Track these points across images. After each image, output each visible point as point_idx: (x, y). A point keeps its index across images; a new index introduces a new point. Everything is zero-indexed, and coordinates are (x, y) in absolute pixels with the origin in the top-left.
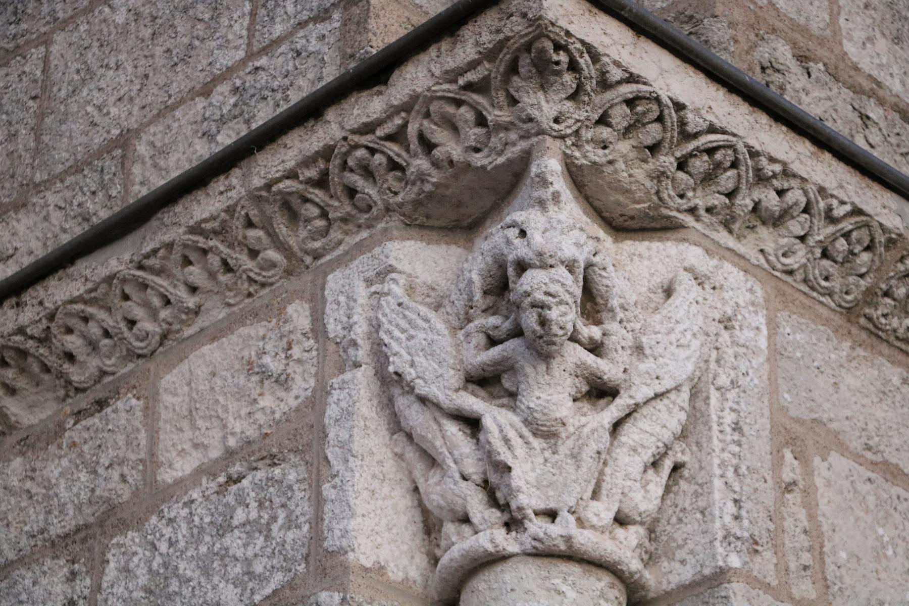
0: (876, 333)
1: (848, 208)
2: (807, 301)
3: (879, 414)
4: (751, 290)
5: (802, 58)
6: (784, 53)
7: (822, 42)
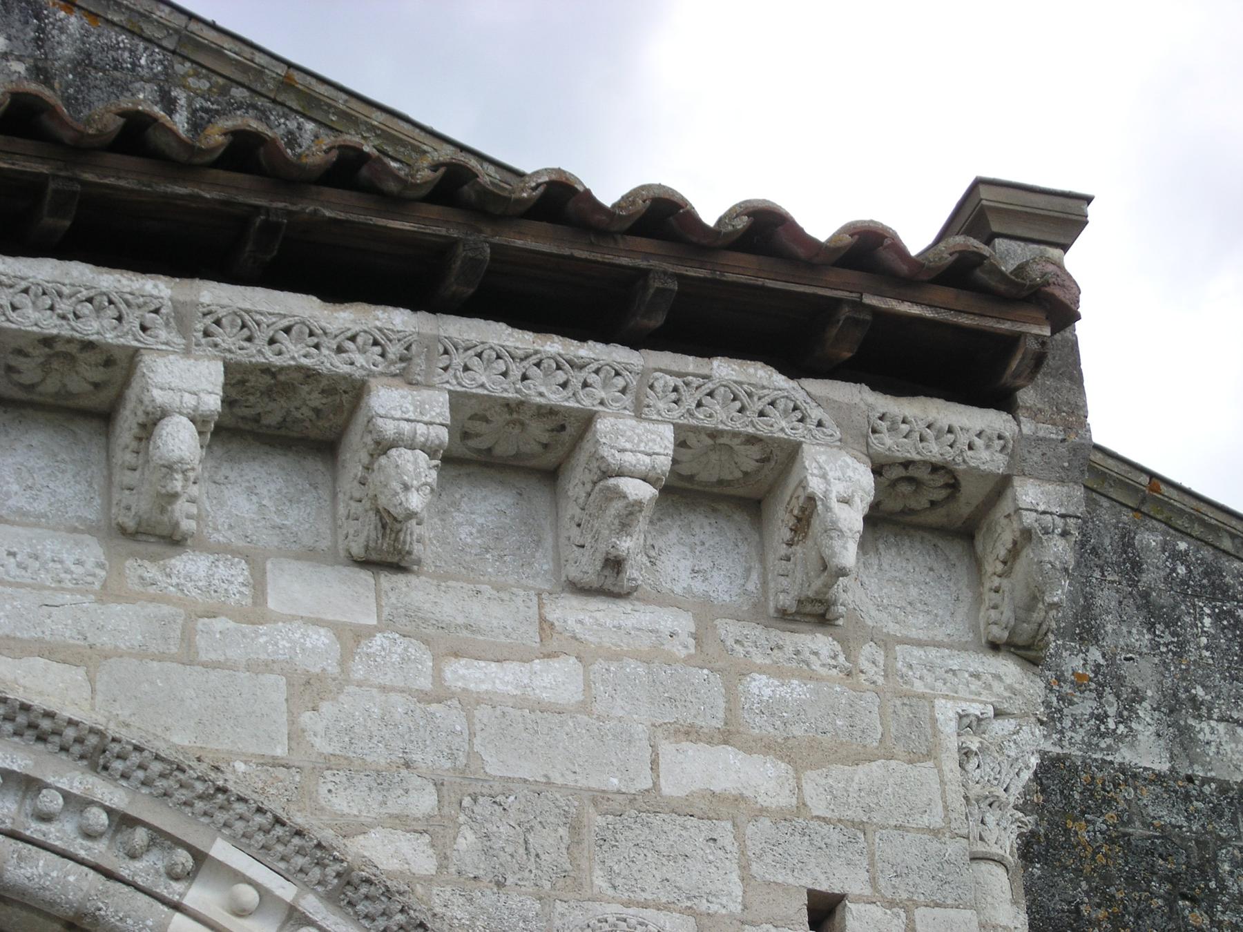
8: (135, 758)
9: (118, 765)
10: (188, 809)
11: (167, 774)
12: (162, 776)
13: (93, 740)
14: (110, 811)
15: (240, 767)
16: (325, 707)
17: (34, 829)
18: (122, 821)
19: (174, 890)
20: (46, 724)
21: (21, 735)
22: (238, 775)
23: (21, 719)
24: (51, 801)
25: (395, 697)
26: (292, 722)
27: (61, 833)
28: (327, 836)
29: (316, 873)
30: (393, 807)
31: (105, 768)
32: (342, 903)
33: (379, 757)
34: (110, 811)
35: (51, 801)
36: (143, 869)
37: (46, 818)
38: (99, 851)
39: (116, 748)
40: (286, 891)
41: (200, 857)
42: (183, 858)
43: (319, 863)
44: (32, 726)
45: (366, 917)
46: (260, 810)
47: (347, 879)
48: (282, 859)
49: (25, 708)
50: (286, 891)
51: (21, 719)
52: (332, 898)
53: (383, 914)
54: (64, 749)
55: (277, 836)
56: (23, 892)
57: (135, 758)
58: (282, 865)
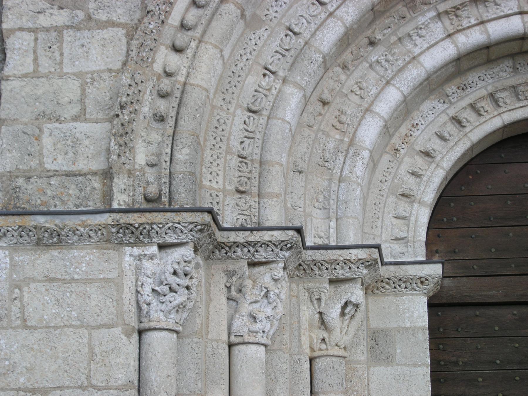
0: (47, 245)
1: (17, 227)
2: (24, 248)
3: (48, 266)
4: (5, 253)
5: (28, 178)
6: (21, 181)
7: (35, 170)
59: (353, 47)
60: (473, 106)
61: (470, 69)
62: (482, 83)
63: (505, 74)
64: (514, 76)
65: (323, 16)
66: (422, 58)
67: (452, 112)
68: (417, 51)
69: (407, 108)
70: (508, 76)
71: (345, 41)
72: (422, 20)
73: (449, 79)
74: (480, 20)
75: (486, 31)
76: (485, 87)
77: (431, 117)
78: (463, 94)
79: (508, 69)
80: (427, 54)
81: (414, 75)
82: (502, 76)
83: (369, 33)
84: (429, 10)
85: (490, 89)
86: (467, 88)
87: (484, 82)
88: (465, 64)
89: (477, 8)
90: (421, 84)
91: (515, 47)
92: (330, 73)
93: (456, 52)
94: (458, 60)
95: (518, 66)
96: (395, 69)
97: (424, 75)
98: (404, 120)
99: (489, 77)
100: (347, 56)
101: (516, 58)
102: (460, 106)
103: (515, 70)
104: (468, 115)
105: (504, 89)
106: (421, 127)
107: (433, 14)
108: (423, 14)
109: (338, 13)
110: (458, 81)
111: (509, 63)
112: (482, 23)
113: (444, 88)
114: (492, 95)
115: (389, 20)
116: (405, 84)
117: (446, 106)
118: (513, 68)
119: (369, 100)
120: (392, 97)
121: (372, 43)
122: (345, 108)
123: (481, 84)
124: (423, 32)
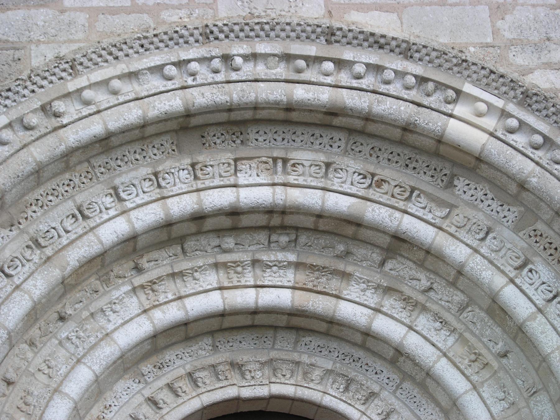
8: (424, 51)
9: (417, 55)
10: (450, 71)
11: (438, 56)
12: (437, 57)
13: (404, 45)
14: (416, 76)
15: (472, 49)
16: (508, 17)
17: (383, 88)
18: (422, 80)
19: (448, 108)
20: (382, 41)
21: (372, 47)
22: (472, 53)
23: (371, 40)
24: (389, 75)
25: (539, 9)
26: (493, 26)
27: (395, 88)
28: (515, 76)
29: (512, 93)
30: (544, 60)
31: (411, 57)
32: (526, 106)
33: (535, 37)
34: (416, 76)
35: (389, 75)
36: (434, 100)
37: (387, 82)
38: (413, 94)
39: (415, 47)
40: (499, 103)
41: (458, 92)
42: (451, 93)
43: (513, 89)
44: (376, 42)
45: (537, 110)
46: (483, 68)
47: (526, 95)
48: (496, 89)
49: (372, 34)
50: (499, 103)
51: (371, 40)
52: (520, 104)
53: (545, 108)
54: (392, 51)
55: (492, 78)
56: (382, 117)
57: (424, 51)
58: (496, 92)
59: (42, 323)
60: (170, 386)
61: (167, 347)
62: (179, 362)
63: (204, 353)
64: (213, 354)
65: (9, 289)
66: (116, 335)
67: (147, 393)
68: (111, 327)
69: (99, 388)
70: (208, 354)
71: (33, 316)
72: (116, 294)
73: (145, 357)
74: (178, 295)
75: (184, 307)
76: (183, 366)
77: (125, 398)
78: (160, 373)
79: (207, 348)
80: (121, 330)
81: (107, 353)
82: (201, 354)
83: (59, 307)
84: (123, 284)
85: (188, 368)
86: (163, 367)
87: (182, 361)
88: (161, 342)
89: (175, 282)
90: (115, 362)
91: (215, 324)
92: (16, 350)
93: (152, 329)
94: (154, 337)
95: (218, 344)
96: (87, 346)
97: (117, 354)
98: (96, 401)
99: (187, 355)
100: (35, 332)
101: (216, 335)
102: (156, 386)
103: (215, 348)
104: (165, 396)
105: (203, 368)
106: (114, 409)
107: (128, 288)
108: (117, 288)
109: (25, 286)
110: (154, 359)
111: (208, 340)
112: (180, 298)
113: (139, 366)
114: (190, 375)
115: (81, 293)
116: (97, 363)
117: (141, 386)
118: (213, 346)
119: (58, 379)
120: (82, 378)
121: (62, 319)
122: (32, 389)
123: (178, 362)
124: (117, 307)
